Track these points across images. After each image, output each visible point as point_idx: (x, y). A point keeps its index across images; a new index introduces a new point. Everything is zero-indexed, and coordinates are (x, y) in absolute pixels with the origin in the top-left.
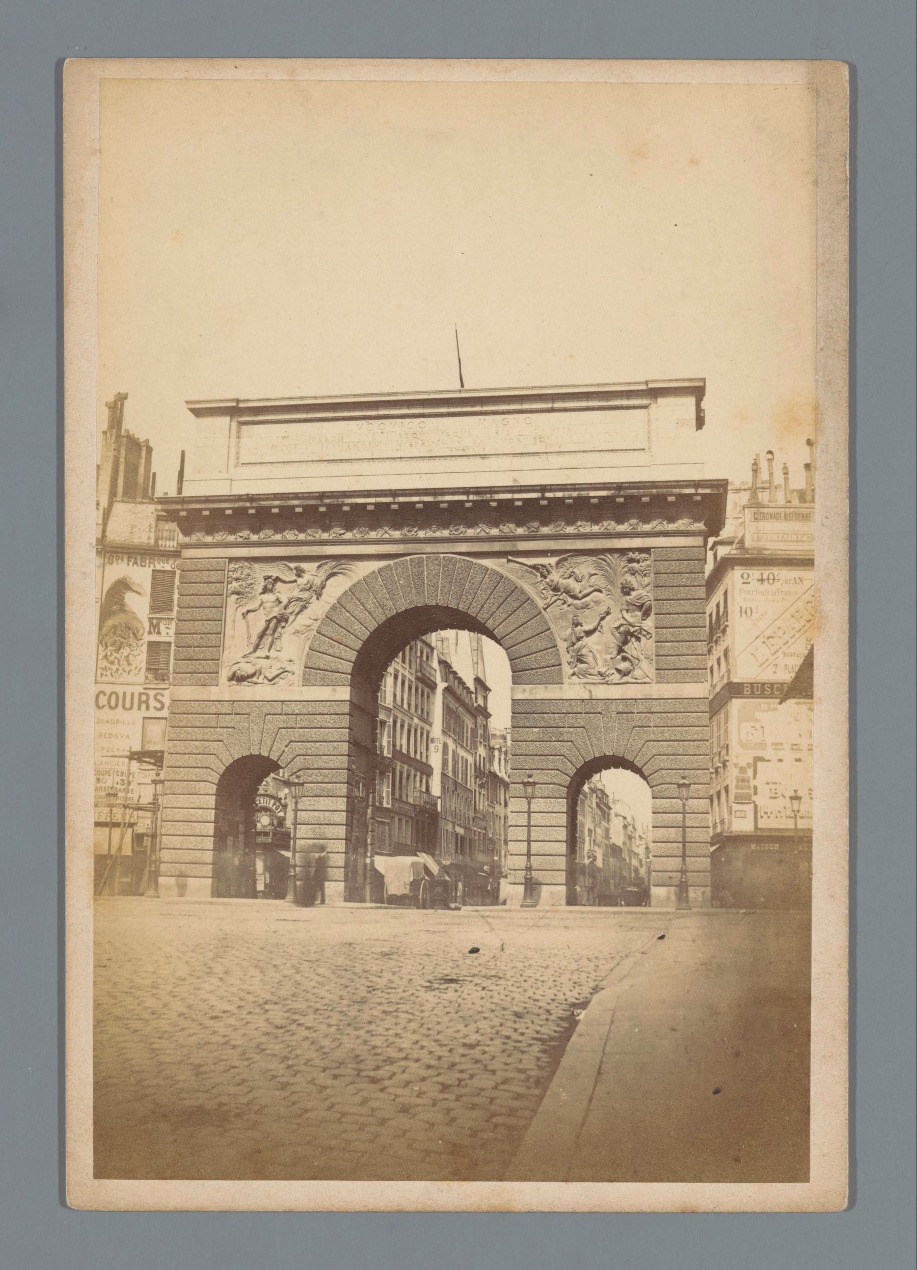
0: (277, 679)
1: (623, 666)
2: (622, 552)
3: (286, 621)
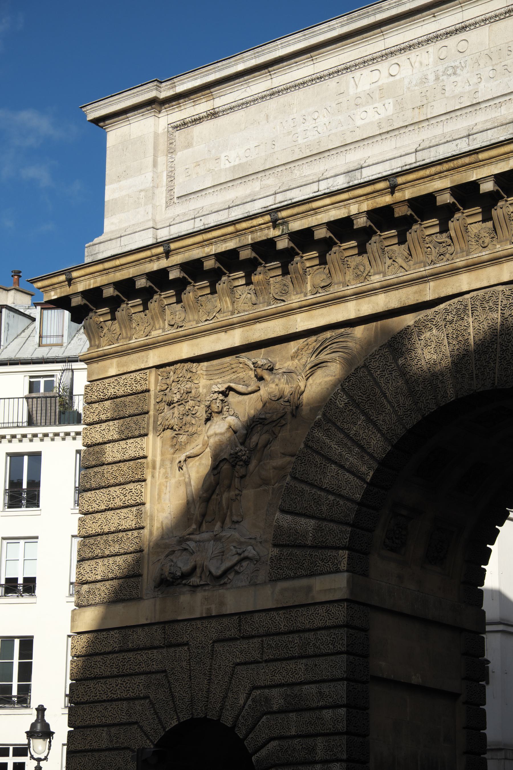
0: (231, 576)
3: (247, 463)
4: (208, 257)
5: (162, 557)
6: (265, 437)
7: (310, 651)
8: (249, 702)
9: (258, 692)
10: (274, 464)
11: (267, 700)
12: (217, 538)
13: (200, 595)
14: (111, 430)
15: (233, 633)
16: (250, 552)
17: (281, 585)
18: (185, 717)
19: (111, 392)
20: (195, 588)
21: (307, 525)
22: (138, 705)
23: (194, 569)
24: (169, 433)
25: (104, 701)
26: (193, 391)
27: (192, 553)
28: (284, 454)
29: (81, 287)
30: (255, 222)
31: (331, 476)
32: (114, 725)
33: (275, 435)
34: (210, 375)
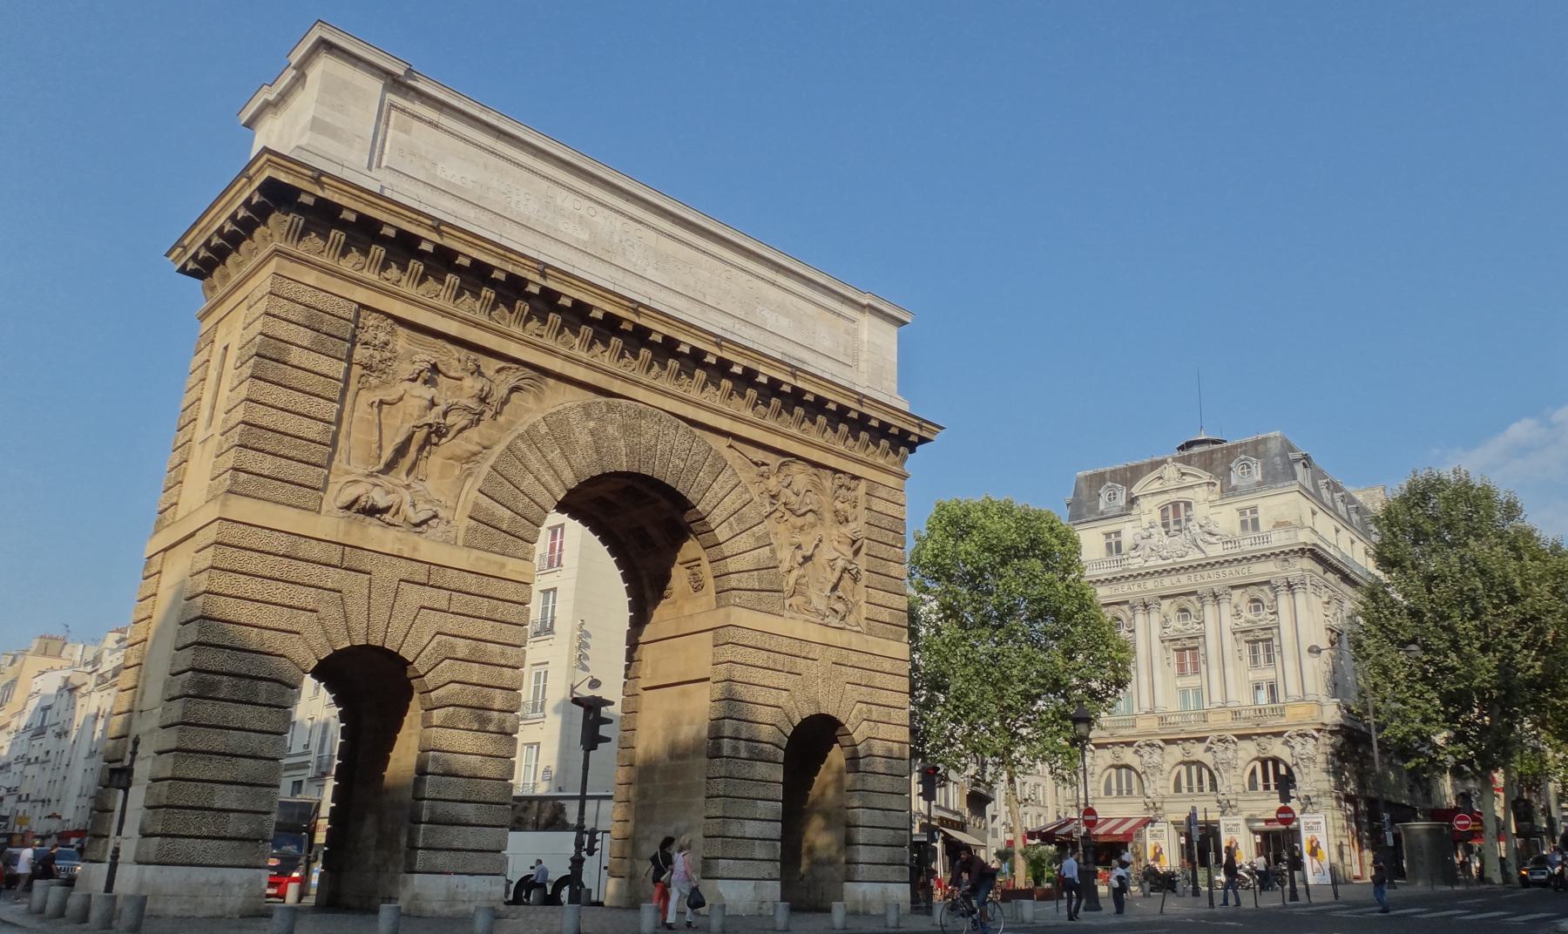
1: (839, 606)
2: (836, 471)
6: (464, 422)
7: (497, 617)
8: (434, 643)
11: (453, 648)
13: (392, 532)
14: (305, 336)
15: (424, 579)
19: (306, 299)
22: (304, 617)
27: (388, 493)
31: (528, 482)
34: (410, 341)
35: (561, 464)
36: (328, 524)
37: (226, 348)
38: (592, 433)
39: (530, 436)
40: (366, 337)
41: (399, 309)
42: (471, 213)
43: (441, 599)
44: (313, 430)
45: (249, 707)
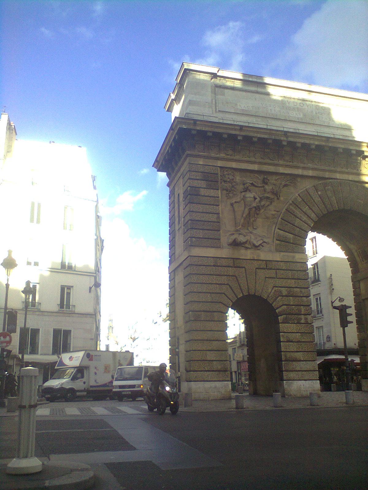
4: (256, 137)
5: (228, 234)
6: (268, 203)
7: (296, 277)
8: (273, 291)
9: (277, 288)
10: (272, 213)
12: (251, 233)
13: (249, 251)
14: (203, 184)
16: (265, 240)
17: (282, 254)
18: (246, 293)
19: (202, 170)
20: (247, 248)
21: (291, 236)
22: (224, 287)
23: (247, 241)
24: (225, 192)
25: (207, 284)
26: (235, 180)
28: (275, 211)
29: (198, 128)
30: (278, 133)
32: (213, 293)
33: (271, 203)
35: (309, 212)
36: (225, 252)
37: (179, 195)
38: (320, 196)
39: (294, 203)
40: (225, 179)
41: (234, 165)
42: (254, 120)
43: (272, 273)
44: (213, 218)
45: (212, 322)
